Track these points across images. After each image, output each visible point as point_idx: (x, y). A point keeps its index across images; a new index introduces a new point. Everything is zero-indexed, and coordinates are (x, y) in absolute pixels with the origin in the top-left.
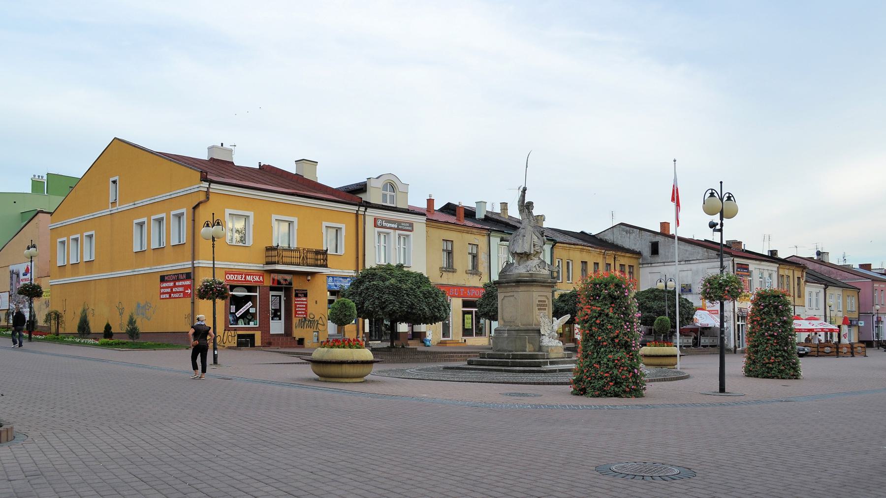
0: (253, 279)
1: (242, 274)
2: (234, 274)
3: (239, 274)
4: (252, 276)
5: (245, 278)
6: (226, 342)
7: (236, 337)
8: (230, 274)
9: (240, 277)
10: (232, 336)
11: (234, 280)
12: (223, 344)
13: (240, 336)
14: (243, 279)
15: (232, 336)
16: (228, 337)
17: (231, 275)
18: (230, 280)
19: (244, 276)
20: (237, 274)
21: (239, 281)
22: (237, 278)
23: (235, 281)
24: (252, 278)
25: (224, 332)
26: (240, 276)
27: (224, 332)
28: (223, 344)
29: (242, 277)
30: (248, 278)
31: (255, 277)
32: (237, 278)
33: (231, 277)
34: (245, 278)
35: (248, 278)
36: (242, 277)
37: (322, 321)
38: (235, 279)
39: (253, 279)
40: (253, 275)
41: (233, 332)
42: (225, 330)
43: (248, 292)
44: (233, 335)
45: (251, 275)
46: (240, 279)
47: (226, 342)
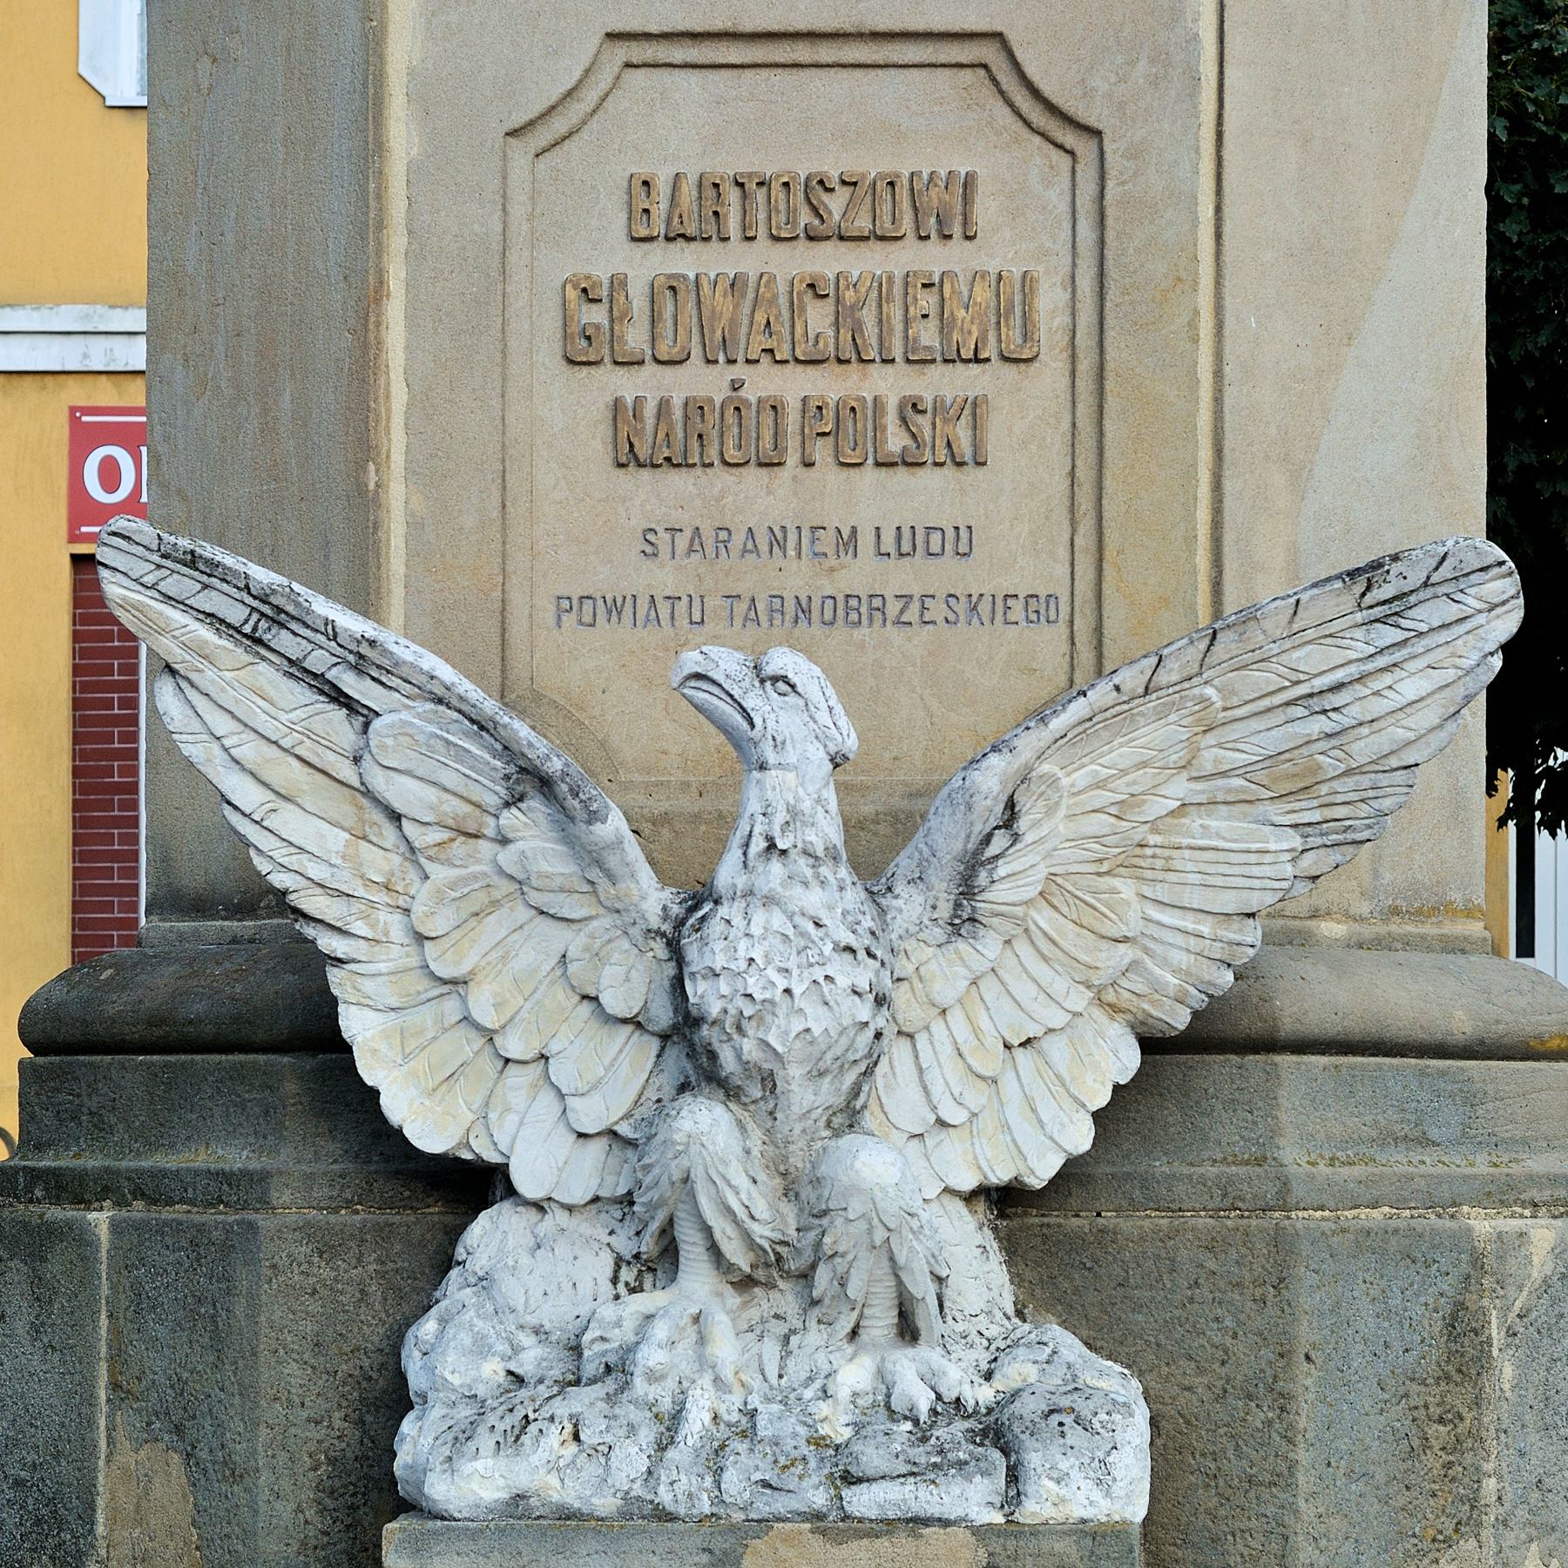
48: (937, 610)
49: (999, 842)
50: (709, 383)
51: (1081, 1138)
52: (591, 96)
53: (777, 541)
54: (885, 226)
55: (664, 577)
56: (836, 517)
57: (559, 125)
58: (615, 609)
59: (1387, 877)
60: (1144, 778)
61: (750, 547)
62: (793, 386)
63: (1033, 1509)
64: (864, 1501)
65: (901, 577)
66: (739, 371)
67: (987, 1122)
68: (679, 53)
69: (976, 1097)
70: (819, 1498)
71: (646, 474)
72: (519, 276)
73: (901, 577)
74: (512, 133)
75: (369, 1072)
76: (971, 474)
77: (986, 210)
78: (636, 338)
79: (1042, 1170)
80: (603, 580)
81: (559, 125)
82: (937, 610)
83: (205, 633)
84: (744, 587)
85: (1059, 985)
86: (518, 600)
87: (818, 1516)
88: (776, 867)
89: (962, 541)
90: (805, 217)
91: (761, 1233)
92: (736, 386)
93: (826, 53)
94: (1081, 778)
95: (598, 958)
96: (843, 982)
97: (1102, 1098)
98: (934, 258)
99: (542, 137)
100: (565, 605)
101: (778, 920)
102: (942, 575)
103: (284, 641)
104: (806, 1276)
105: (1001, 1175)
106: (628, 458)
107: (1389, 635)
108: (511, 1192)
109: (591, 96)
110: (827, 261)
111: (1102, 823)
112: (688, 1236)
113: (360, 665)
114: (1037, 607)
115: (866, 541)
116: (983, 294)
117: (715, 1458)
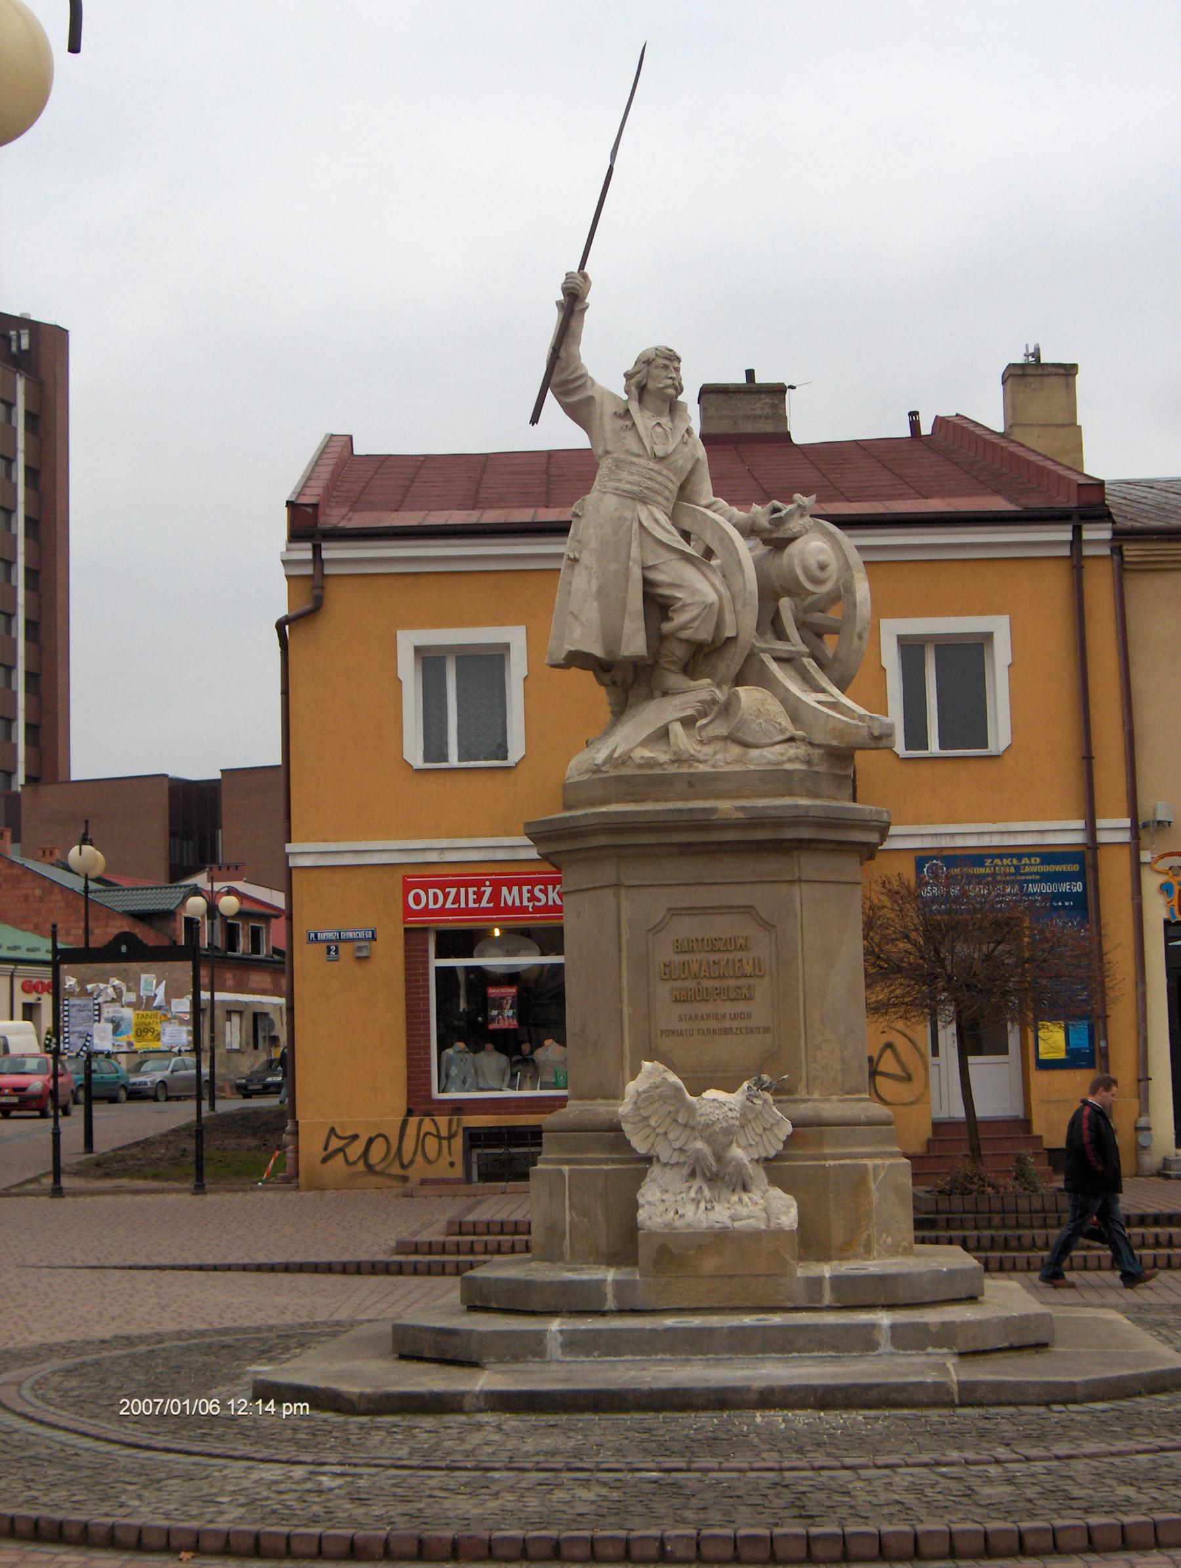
0: (533, 898)
1: (479, 884)
2: (442, 886)
3: (467, 884)
4: (525, 888)
5: (495, 896)
6: (412, 1162)
7: (458, 1143)
8: (425, 887)
9: (472, 897)
10: (439, 1137)
11: (443, 911)
12: (396, 1170)
13: (475, 1138)
14: (484, 904)
15: (439, 1137)
16: (420, 1141)
17: (431, 891)
18: (426, 911)
19: (488, 890)
20: (458, 885)
21: (468, 911)
22: (457, 900)
23: (452, 912)
24: (526, 895)
25: (404, 1124)
26: (471, 890)
27: (404, 1124)
28: (396, 1170)
29: (479, 896)
30: (509, 896)
31: (545, 892)
32: (457, 900)
33: (430, 899)
34: (495, 896)
35: (509, 896)
36: (479, 896)
37: (899, 1061)
38: (449, 905)
39: (533, 898)
40: (533, 883)
41: (442, 1121)
42: (410, 1112)
43: (543, 954)
44: (444, 1133)
45: (520, 883)
46: (471, 905)
47: (412, 1162)
48: (744, 1031)
50: (690, 984)
51: (780, 1146)
52: (665, 922)
53: (708, 1016)
54: (729, 948)
55: (685, 1026)
57: (658, 928)
58: (673, 1032)
61: (702, 1018)
66: (699, 980)
67: (760, 1144)
68: (684, 912)
69: (757, 1139)
71: (679, 1004)
74: (649, 931)
75: (628, 1136)
79: (772, 1153)
81: (658, 928)
82: (744, 1031)
89: (749, 1016)
91: (714, 1169)
92: (699, 984)
95: (677, 1112)
98: (739, 955)
100: (662, 1032)
102: (743, 1023)
104: (724, 1177)
105: (764, 1155)
106: (676, 1001)
108: (658, 1160)
109: (665, 922)
110: (715, 957)
112: (698, 1170)
114: (766, 1030)
116: (751, 962)
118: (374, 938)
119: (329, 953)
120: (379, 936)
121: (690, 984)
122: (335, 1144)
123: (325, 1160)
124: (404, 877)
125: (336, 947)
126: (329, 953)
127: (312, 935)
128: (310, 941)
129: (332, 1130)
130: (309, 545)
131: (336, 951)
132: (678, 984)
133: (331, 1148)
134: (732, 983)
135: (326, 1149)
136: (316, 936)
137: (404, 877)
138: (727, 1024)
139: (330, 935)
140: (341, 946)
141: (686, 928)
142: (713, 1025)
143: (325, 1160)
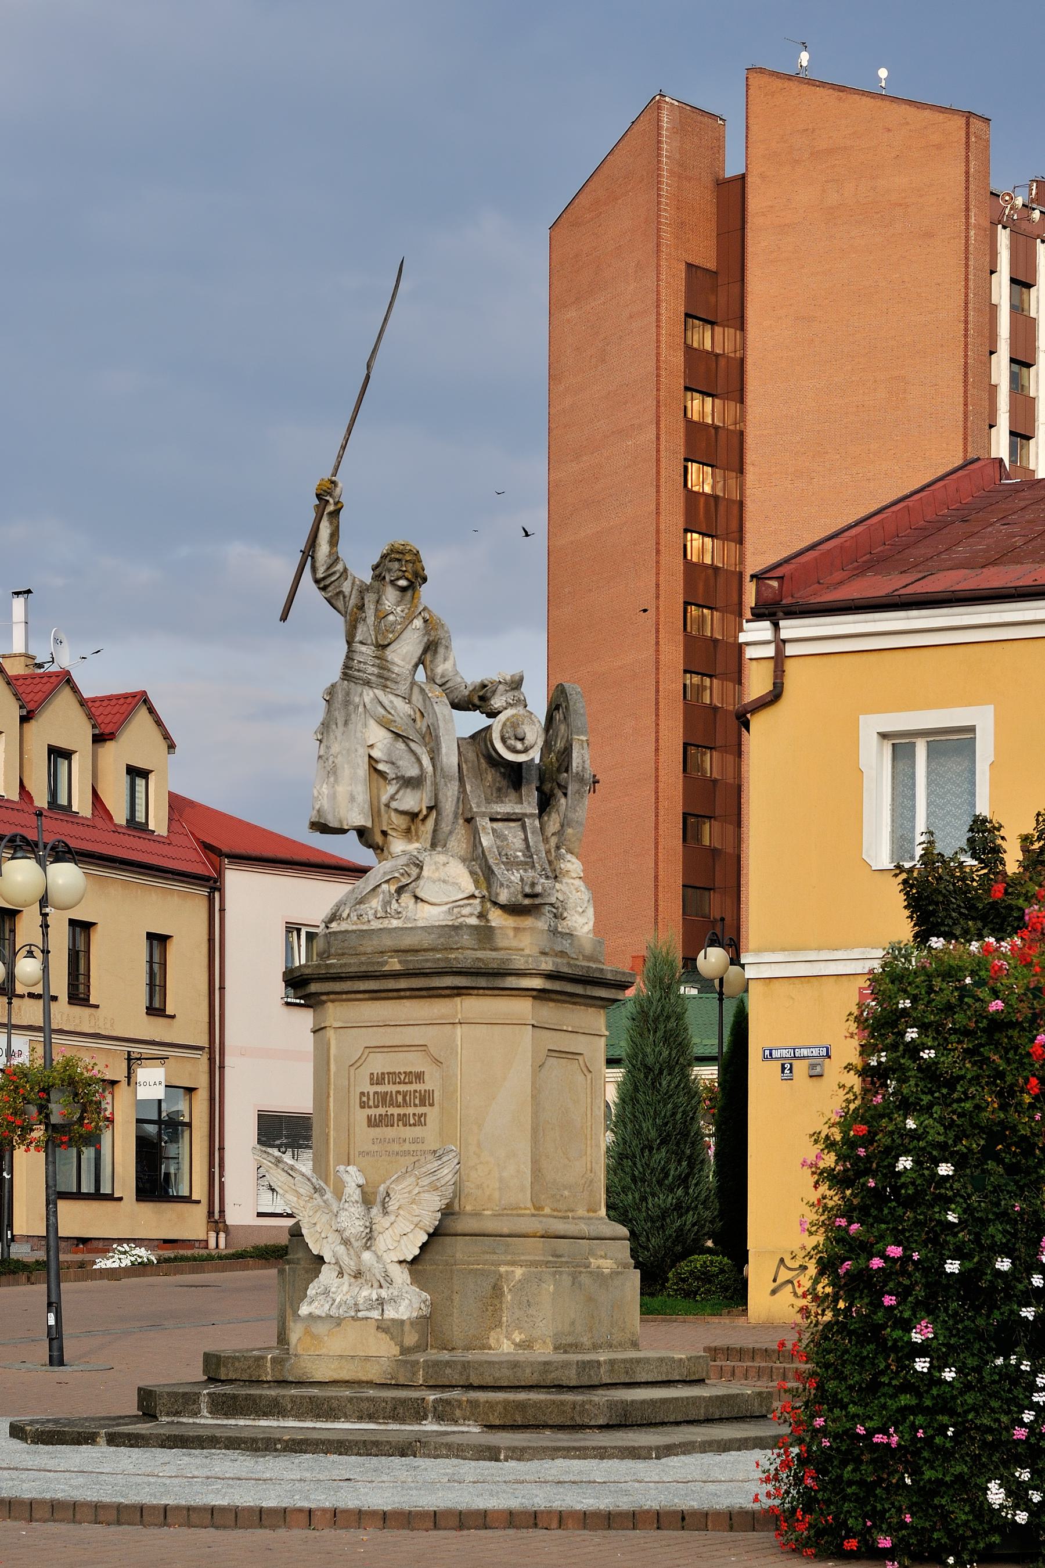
48: (419, 1153)
49: (387, 1199)
52: (363, 1058)
55: (375, 1148)
56: (403, 1136)
57: (358, 1064)
59: (503, 1202)
60: (411, 1187)
62: (395, 1111)
63: (386, 1317)
64: (360, 1314)
65: (413, 1147)
66: (387, 1109)
70: (353, 1314)
72: (352, 1093)
73: (413, 1147)
76: (424, 1127)
77: (426, 1077)
78: (371, 1103)
80: (366, 1148)
81: (358, 1064)
82: (419, 1153)
83: (270, 1164)
84: (387, 1149)
85: (408, 1224)
86: (352, 1153)
87: (353, 1317)
88: (347, 1204)
90: (398, 1080)
93: (400, 1049)
94: (400, 1187)
96: (357, 1224)
97: (420, 1244)
99: (356, 1066)
100: (360, 1153)
101: (347, 1213)
103: (280, 1165)
107: (440, 1162)
109: (363, 1058)
110: (402, 1088)
111: (406, 1195)
113: (292, 1169)
115: (407, 1140)
117: (339, 1307)
118: (828, 1056)
119: (783, 1072)
120: (832, 1053)
121: (381, 1111)
122: (784, 1275)
123: (774, 1292)
124: (860, 988)
125: (791, 1065)
126: (783, 1072)
127: (767, 1052)
128: (765, 1058)
129: (782, 1260)
130: (767, 624)
131: (791, 1070)
132: (372, 1112)
133: (779, 1281)
134: (410, 1111)
135: (775, 1280)
136: (771, 1054)
137: (860, 988)
138: (407, 1147)
139: (785, 1053)
140: (795, 1063)
141: (379, 1064)
142: (396, 1147)
143: (774, 1292)
